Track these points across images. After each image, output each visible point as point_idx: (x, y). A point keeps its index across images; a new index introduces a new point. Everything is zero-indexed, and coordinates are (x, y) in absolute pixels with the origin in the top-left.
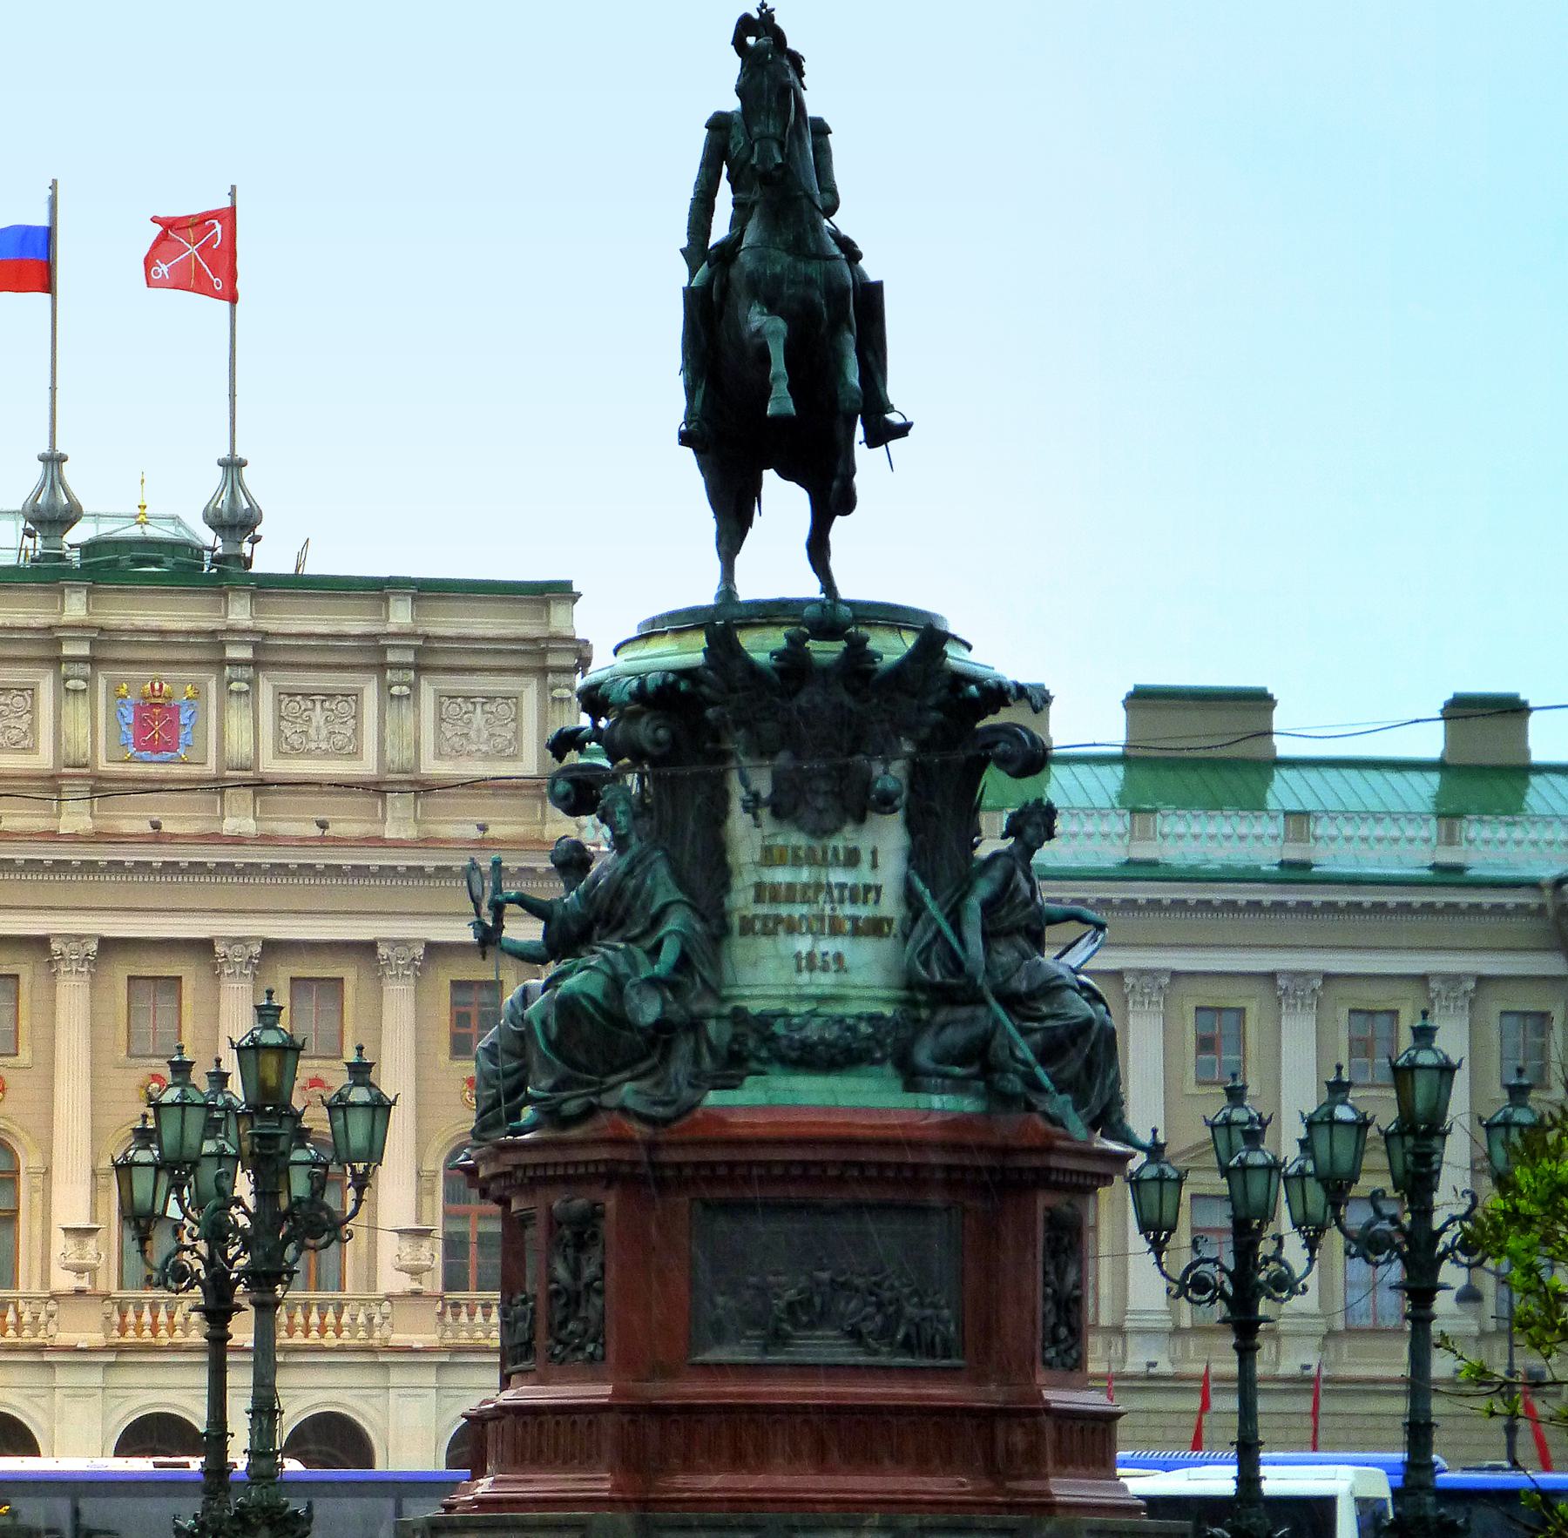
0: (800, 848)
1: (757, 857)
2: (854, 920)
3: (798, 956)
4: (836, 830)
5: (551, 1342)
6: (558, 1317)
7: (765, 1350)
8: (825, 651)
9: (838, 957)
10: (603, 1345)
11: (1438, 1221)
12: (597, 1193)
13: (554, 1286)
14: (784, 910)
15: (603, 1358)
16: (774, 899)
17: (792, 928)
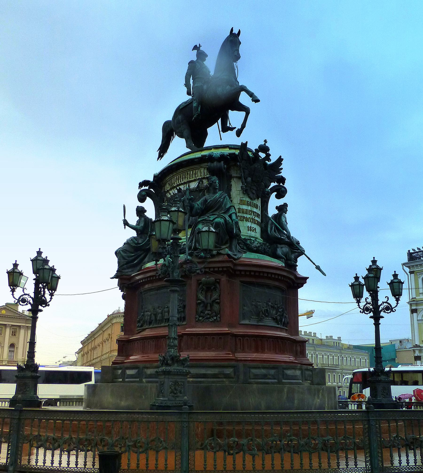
0: (248, 202)
1: (239, 202)
2: (257, 220)
3: (248, 227)
4: (255, 199)
5: (197, 316)
6: (200, 310)
7: (258, 322)
8: (262, 155)
9: (255, 229)
10: (220, 317)
11: (379, 303)
12: (219, 276)
13: (199, 301)
14: (245, 215)
15: (220, 320)
16: (243, 213)
17: (247, 220)
